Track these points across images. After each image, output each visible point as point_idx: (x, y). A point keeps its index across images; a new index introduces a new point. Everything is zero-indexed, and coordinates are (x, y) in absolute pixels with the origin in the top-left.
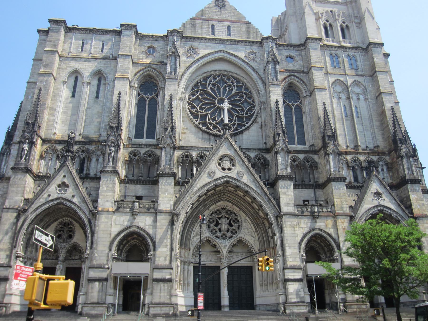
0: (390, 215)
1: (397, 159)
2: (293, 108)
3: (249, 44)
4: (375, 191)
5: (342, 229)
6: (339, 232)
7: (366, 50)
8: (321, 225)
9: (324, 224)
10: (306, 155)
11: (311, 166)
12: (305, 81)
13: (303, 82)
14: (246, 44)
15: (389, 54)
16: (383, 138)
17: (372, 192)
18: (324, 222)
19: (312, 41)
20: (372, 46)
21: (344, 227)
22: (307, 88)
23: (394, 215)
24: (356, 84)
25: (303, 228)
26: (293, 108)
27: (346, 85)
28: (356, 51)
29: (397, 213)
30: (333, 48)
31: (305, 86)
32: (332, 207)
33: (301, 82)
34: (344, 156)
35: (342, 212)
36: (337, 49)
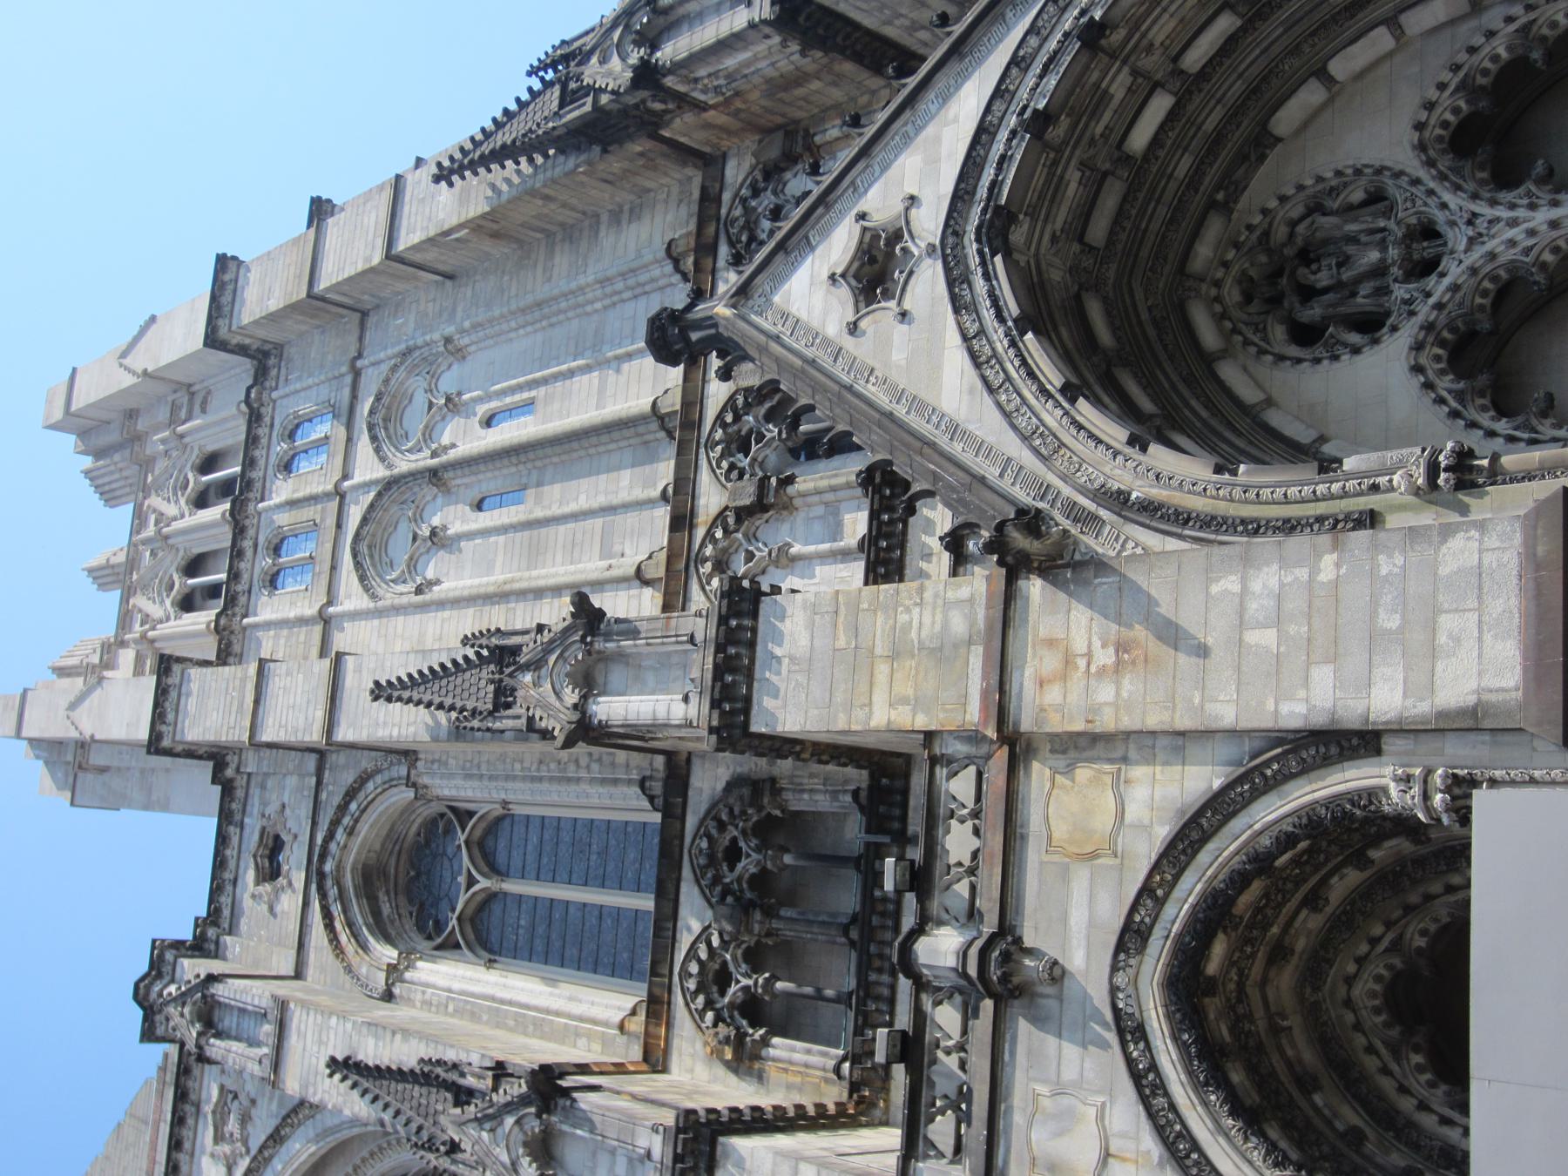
0: (1038, 123)
1: (701, 107)
2: (483, 883)
3: (190, 1121)
4: (844, 292)
5: (1128, 684)
6: (1154, 721)
7: (266, 354)
8: (1091, 924)
9: (1081, 878)
10: (687, 872)
11: (768, 831)
12: (349, 778)
13: (351, 794)
14: (187, 1145)
15: (312, 199)
16: (635, 213)
17: (853, 328)
18: (1065, 875)
19: (170, 717)
20: (223, 333)
21: (1105, 657)
22: (378, 771)
23: (1035, 92)
24: (386, 420)
25: (1106, 1156)
26: (483, 883)
27: (379, 495)
28: (267, 420)
29: (1018, 62)
30: (242, 565)
31: (370, 786)
32: (948, 761)
33: (353, 806)
34: (700, 533)
35: (976, 660)
36: (247, 544)
